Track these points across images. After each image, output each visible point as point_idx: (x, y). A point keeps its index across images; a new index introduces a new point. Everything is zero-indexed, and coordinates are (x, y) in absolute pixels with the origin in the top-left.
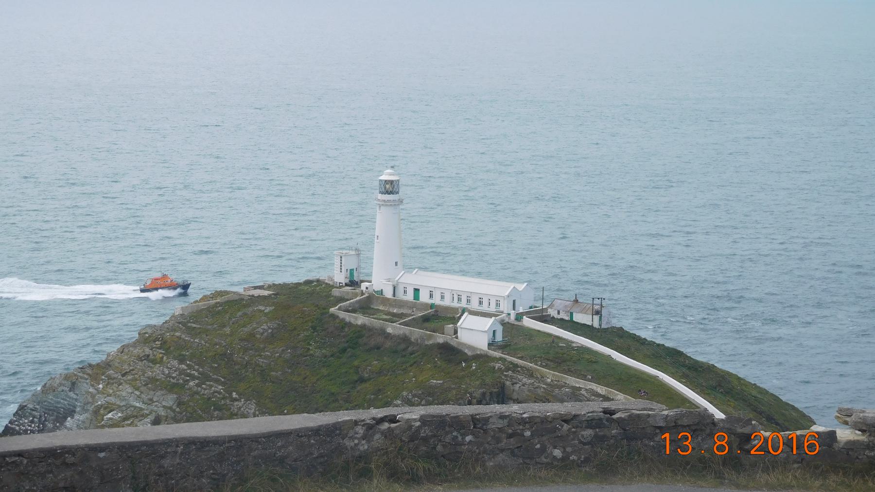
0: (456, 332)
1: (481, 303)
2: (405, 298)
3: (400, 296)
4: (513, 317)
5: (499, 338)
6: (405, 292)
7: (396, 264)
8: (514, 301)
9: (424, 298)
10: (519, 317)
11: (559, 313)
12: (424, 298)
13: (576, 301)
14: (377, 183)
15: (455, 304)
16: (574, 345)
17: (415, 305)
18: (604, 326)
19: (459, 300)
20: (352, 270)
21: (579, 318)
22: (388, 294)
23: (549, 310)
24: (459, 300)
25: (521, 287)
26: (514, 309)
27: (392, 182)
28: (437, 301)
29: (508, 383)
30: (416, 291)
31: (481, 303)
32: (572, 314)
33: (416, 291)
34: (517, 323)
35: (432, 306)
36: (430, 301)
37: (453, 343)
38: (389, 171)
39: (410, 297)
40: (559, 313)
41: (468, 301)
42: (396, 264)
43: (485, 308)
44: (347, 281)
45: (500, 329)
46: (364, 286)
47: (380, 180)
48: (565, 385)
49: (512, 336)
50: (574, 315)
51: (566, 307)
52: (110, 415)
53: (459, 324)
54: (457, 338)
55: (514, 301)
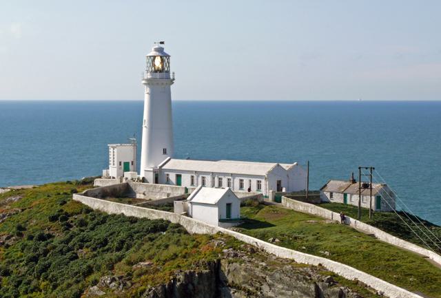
10: (277, 199)
11: (331, 196)
20: (124, 163)
25: (286, 166)
30: (179, 177)
31: (241, 186)
32: (345, 195)
33: (179, 177)
37: (184, 221)
40: (331, 196)
42: (165, 152)
50: (348, 196)
51: (341, 188)
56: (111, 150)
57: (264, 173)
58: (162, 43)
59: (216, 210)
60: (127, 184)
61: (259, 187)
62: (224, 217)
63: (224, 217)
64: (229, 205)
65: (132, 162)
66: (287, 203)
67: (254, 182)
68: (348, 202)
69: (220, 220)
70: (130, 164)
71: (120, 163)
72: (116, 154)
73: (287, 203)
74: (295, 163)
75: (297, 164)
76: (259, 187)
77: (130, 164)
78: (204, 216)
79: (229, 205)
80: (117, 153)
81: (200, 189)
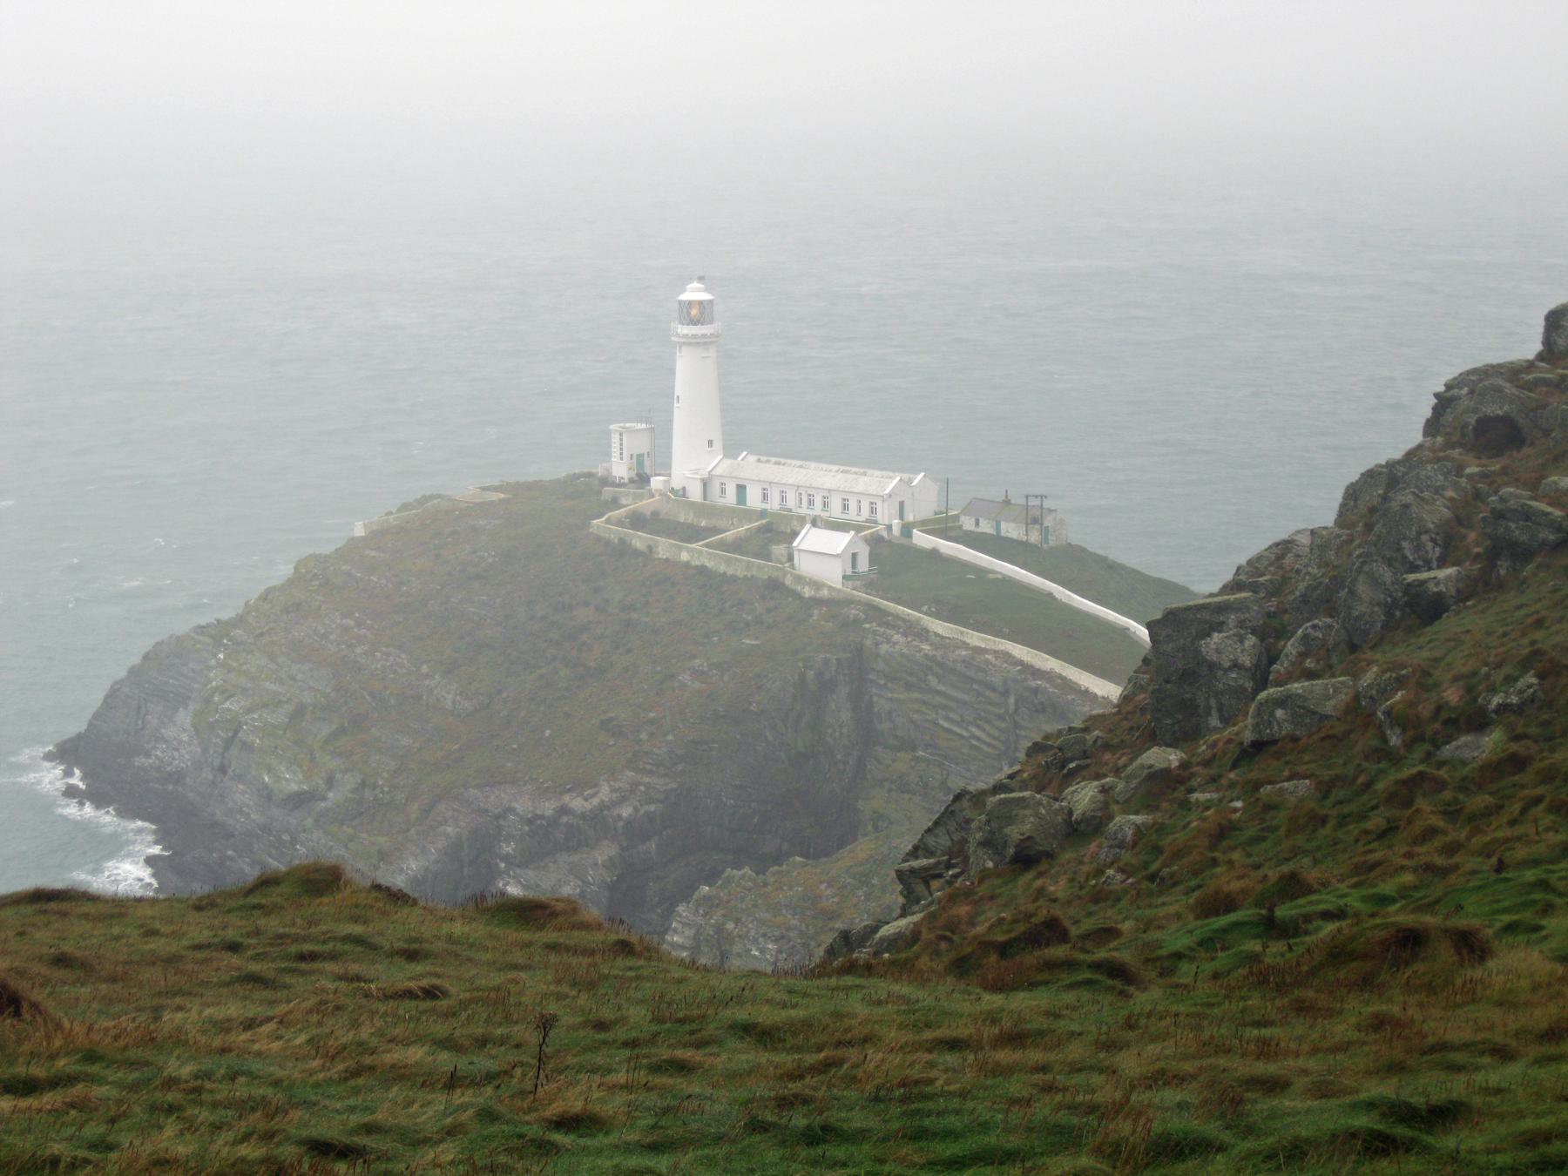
0: (791, 559)
1: (845, 507)
2: (721, 501)
3: (716, 498)
4: (896, 531)
5: (863, 565)
6: (723, 491)
7: (710, 443)
8: (902, 504)
9: (754, 500)
10: (907, 530)
11: (977, 524)
12: (754, 500)
13: (1007, 502)
14: (676, 306)
15: (804, 511)
16: (991, 576)
17: (741, 512)
18: (1052, 542)
19: (811, 503)
20: (640, 456)
21: (1011, 530)
22: (695, 494)
23: (962, 518)
26: (901, 517)
27: (701, 303)
28: (774, 505)
29: (868, 642)
30: (741, 489)
31: (845, 507)
33: (741, 489)
34: (904, 541)
35: (763, 514)
36: (764, 506)
38: (696, 285)
39: (731, 498)
40: (977, 524)
41: (825, 505)
42: (710, 443)
43: (852, 515)
44: (633, 474)
45: (864, 552)
46: (656, 482)
48: (966, 645)
49: (890, 560)
50: (1003, 525)
52: (227, 705)
54: (793, 567)
55: (902, 504)
58: (701, 279)
61: (873, 511)
62: (849, 572)
63: (849, 572)
64: (854, 556)
68: (1003, 533)
73: (922, 540)
76: (873, 511)
79: (854, 556)
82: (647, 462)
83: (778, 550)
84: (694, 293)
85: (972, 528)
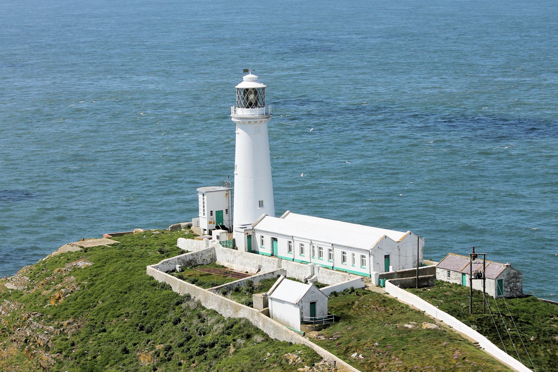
0: (266, 305)
1: (344, 259)
8: (387, 257)
11: (449, 275)
16: (427, 325)
19: (320, 254)
20: (217, 212)
23: (438, 270)
24: (320, 254)
25: (396, 235)
31: (344, 259)
33: (275, 239)
40: (449, 275)
42: (261, 204)
47: (238, 89)
53: (268, 293)
56: (200, 196)
57: (369, 246)
59: (298, 310)
60: (213, 249)
62: (307, 318)
63: (307, 318)
64: (313, 304)
65: (227, 210)
66: (393, 291)
67: (358, 255)
69: (303, 322)
70: (224, 212)
71: (211, 212)
72: (205, 201)
73: (393, 291)
74: (408, 232)
75: (410, 234)
77: (224, 212)
78: (285, 313)
79: (313, 304)
80: (207, 200)
81: (282, 280)
82: (225, 217)
83: (257, 298)
84: (248, 82)
85: (445, 279)
